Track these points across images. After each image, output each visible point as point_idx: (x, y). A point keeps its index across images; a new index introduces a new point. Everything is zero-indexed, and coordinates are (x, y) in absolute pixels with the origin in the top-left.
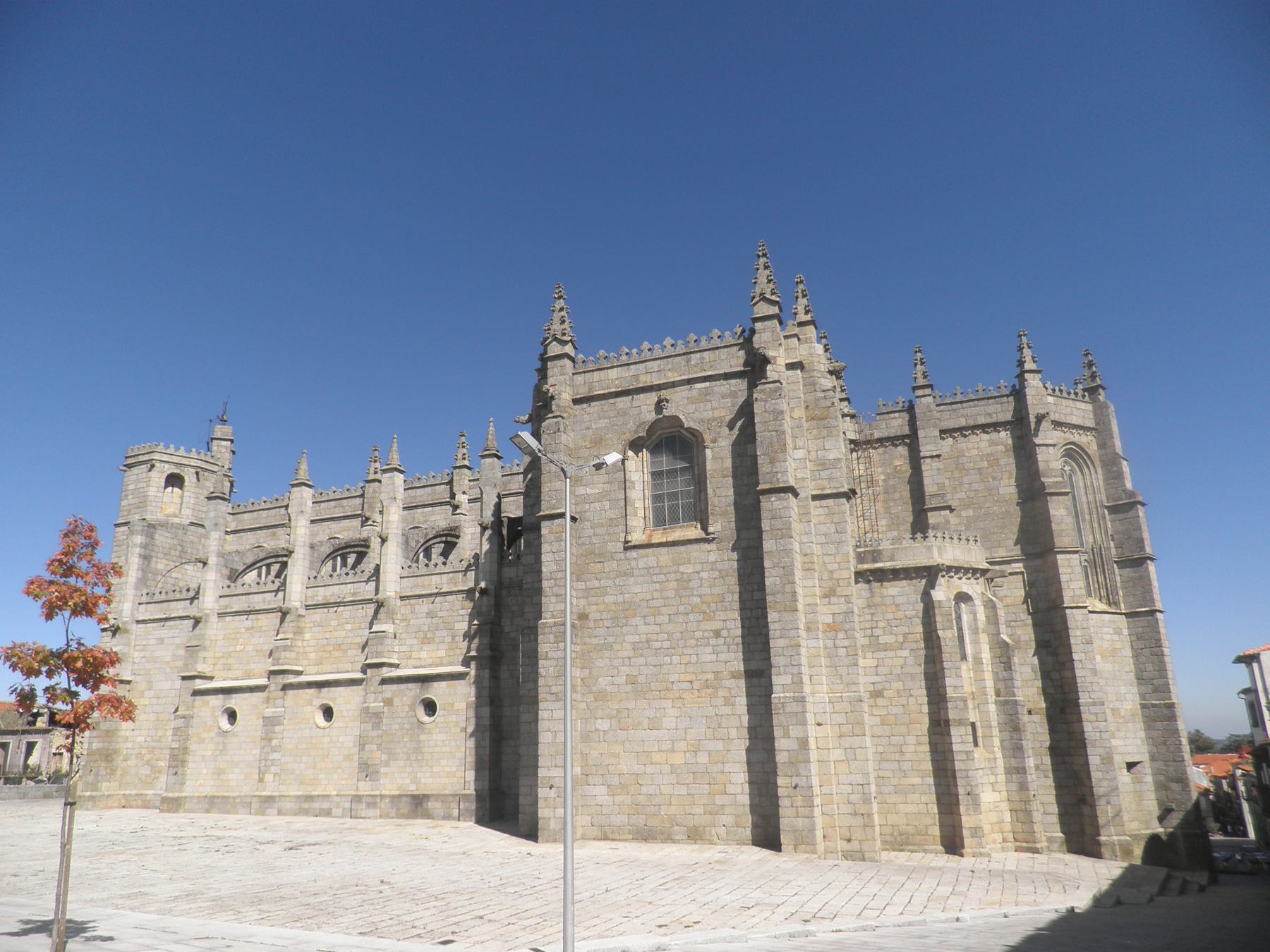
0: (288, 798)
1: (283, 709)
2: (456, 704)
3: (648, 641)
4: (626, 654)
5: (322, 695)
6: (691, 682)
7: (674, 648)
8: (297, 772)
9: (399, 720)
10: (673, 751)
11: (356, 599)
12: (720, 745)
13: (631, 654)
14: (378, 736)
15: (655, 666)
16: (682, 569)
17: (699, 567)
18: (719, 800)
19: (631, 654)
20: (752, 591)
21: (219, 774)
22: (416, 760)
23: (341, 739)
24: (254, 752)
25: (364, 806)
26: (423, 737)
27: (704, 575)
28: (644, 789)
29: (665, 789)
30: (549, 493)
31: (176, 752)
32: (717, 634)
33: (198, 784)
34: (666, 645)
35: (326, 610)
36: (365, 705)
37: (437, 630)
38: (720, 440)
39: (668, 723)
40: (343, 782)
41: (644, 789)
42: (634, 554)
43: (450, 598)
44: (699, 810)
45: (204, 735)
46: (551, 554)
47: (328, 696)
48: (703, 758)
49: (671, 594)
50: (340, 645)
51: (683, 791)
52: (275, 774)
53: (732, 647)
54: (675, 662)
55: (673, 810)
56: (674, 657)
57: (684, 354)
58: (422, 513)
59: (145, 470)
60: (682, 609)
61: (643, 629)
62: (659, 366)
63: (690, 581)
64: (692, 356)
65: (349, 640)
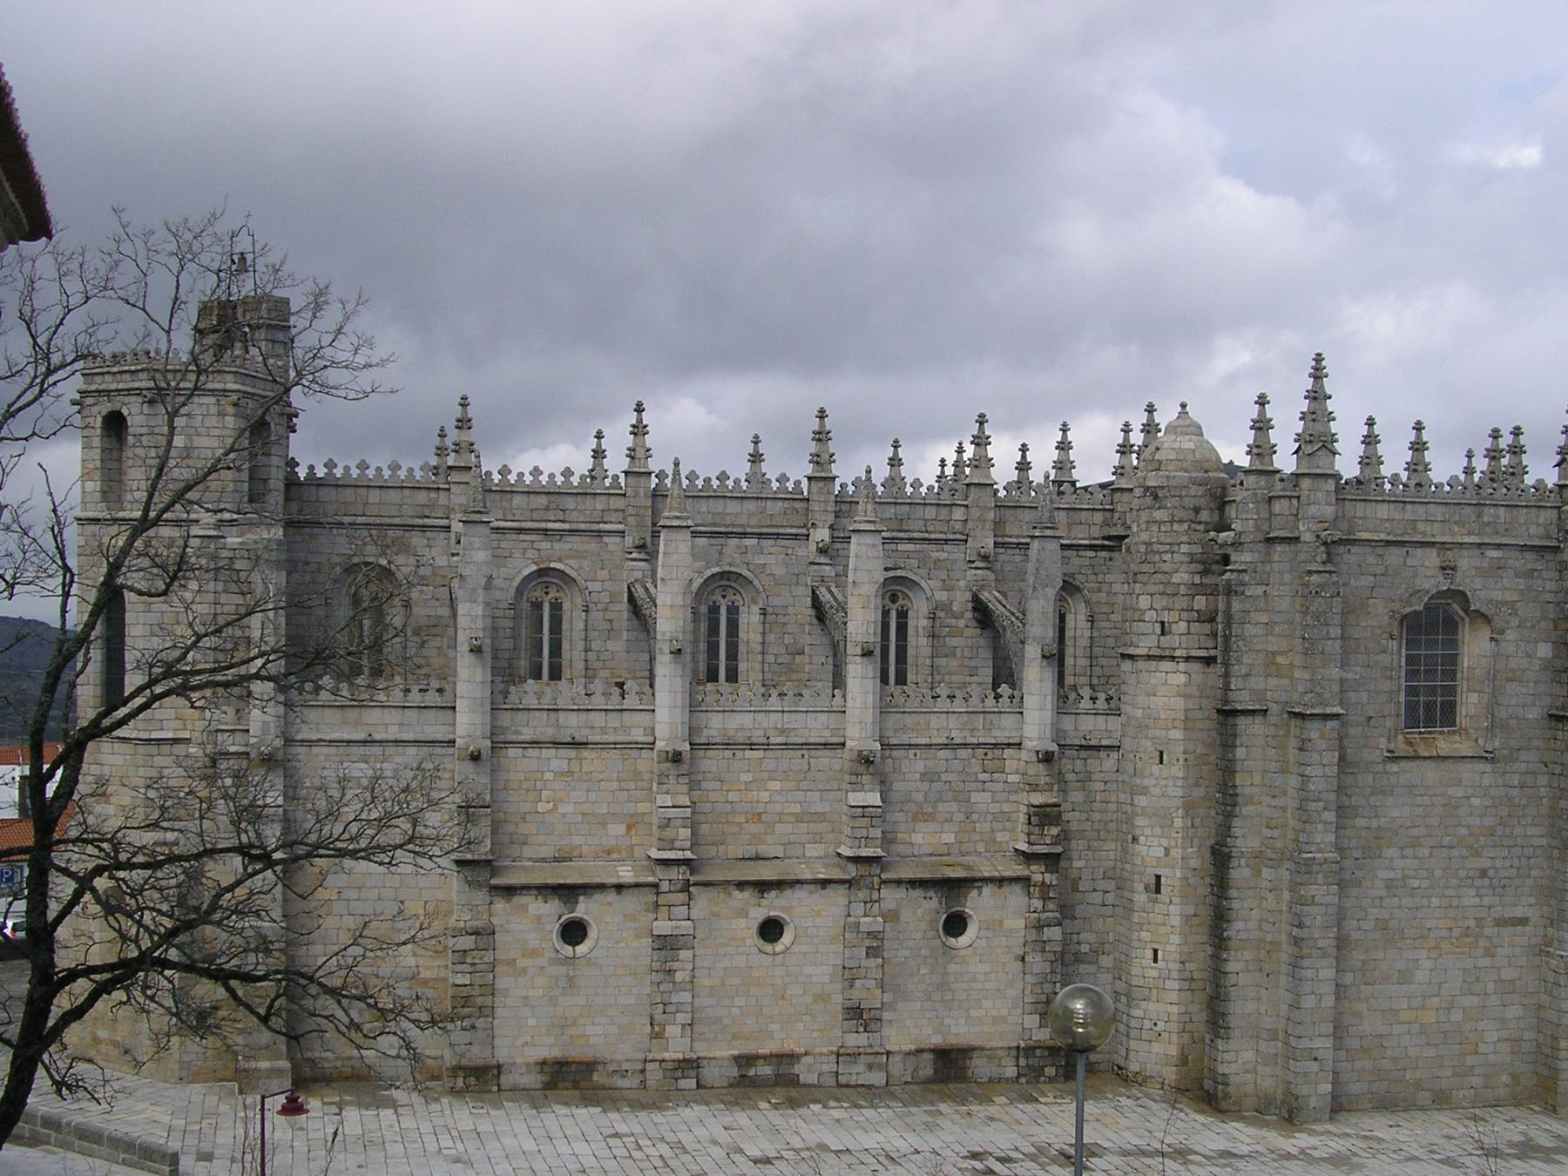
0: (713, 1063)
1: (689, 923)
2: (1006, 922)
3: (1405, 877)
4: (1377, 893)
5: (764, 902)
6: (1451, 929)
7: (1433, 889)
8: (726, 1021)
9: (911, 943)
10: (1423, 1008)
11: (792, 740)
12: (1474, 1001)
13: (1383, 893)
14: (877, 966)
15: (1410, 909)
16: (1450, 791)
17: (1470, 791)
18: (1470, 1060)
19: (1383, 893)
20: (1526, 825)
21: (563, 1027)
22: (943, 1001)
23: (807, 970)
24: (635, 991)
25: (861, 1068)
26: (952, 968)
27: (1475, 801)
28: (1389, 1053)
29: (1413, 1052)
30: (1323, 683)
31: (465, 992)
32: (1483, 873)
33: (519, 1042)
34: (1425, 884)
35: (729, 754)
36: (849, 919)
37: (940, 800)
38: (1508, 631)
39: (1421, 976)
40: (815, 1035)
41: (1389, 1053)
42: (1395, 767)
43: (962, 753)
44: (1449, 1073)
45: (521, 963)
46: (1320, 767)
47: (773, 904)
48: (1456, 1016)
49: (1434, 821)
50: (760, 814)
51: (1432, 1052)
52: (683, 1026)
53: (1498, 890)
54: (1433, 905)
55: (1418, 1074)
56: (1433, 899)
57: (1476, 505)
58: (739, 547)
59: (213, 410)
60: (1446, 841)
61: (1399, 863)
62: (1443, 515)
63: (1459, 807)
64: (1486, 510)
65: (778, 808)
